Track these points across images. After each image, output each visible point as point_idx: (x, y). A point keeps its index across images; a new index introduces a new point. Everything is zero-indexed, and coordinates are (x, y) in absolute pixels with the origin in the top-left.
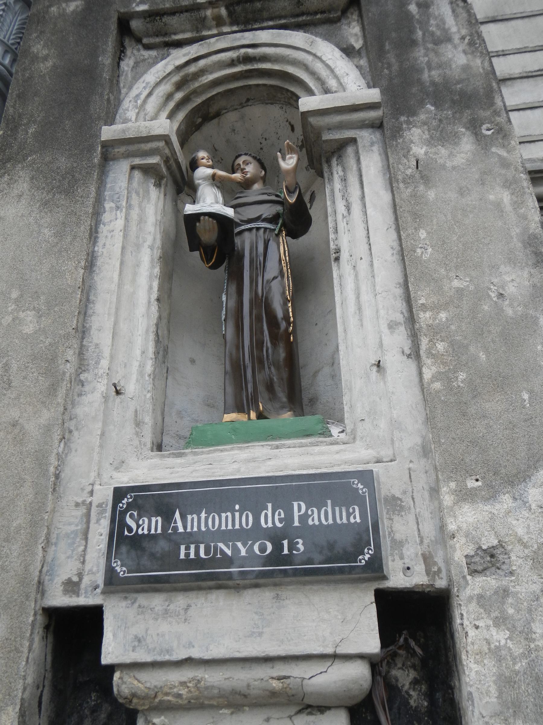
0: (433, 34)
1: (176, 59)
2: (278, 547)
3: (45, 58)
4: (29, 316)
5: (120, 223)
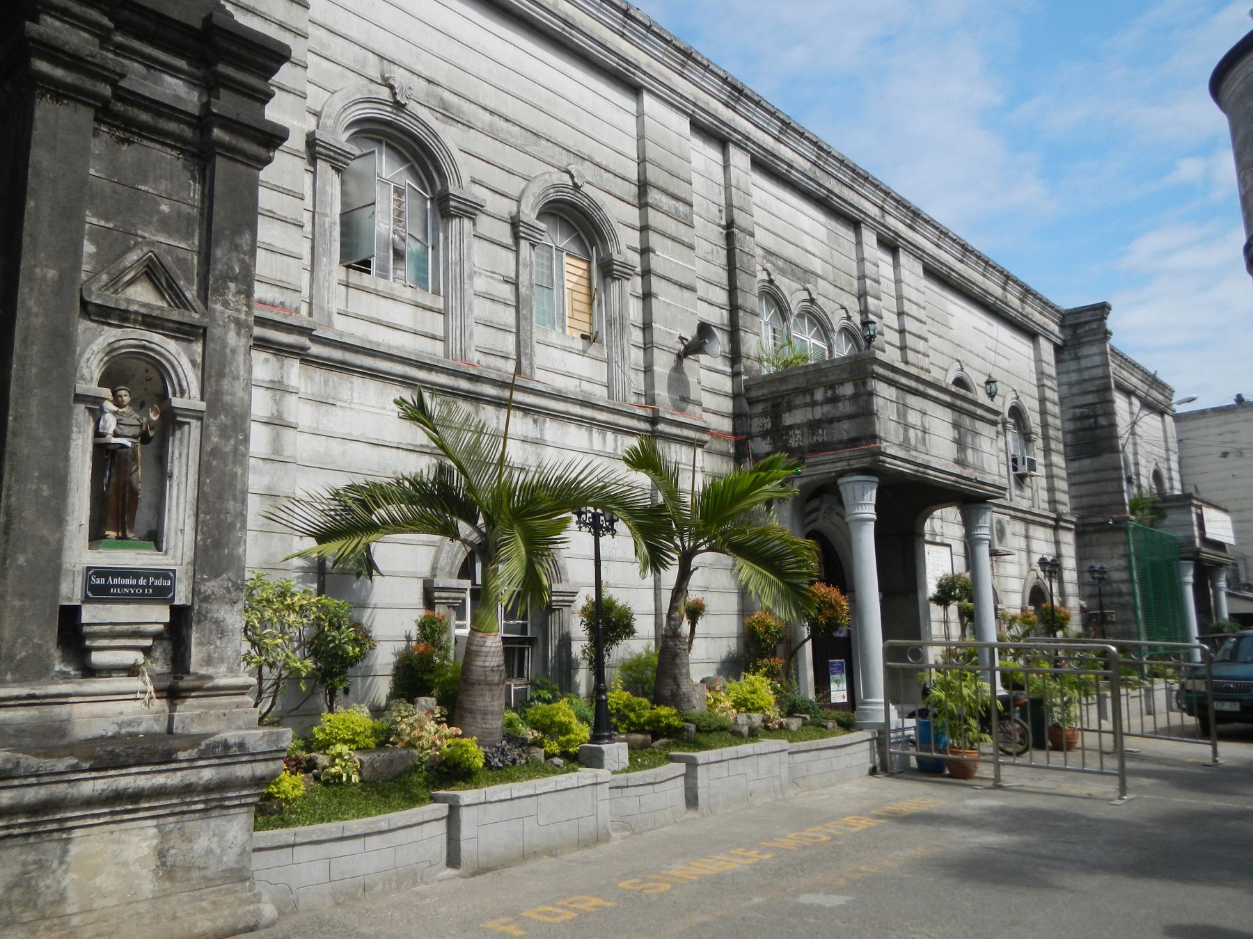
0: (232, 372)
1: (108, 337)
2: (144, 591)
3: (37, 315)
4: (45, 487)
5: (80, 441)
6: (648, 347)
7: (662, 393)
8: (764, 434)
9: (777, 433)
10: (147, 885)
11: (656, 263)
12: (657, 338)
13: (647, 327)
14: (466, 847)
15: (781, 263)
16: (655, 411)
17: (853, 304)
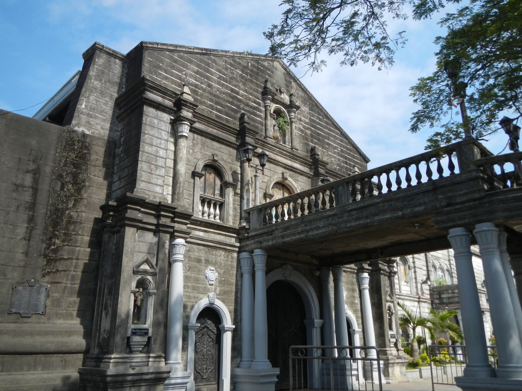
6: (416, 282)
7: (420, 292)
8: (437, 299)
9: (440, 298)
10: (400, 374)
11: (416, 265)
12: (418, 281)
13: (416, 278)
14: (423, 376)
15: (434, 257)
16: (419, 296)
17: (447, 263)
